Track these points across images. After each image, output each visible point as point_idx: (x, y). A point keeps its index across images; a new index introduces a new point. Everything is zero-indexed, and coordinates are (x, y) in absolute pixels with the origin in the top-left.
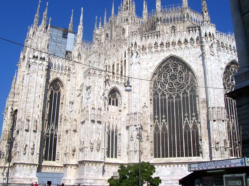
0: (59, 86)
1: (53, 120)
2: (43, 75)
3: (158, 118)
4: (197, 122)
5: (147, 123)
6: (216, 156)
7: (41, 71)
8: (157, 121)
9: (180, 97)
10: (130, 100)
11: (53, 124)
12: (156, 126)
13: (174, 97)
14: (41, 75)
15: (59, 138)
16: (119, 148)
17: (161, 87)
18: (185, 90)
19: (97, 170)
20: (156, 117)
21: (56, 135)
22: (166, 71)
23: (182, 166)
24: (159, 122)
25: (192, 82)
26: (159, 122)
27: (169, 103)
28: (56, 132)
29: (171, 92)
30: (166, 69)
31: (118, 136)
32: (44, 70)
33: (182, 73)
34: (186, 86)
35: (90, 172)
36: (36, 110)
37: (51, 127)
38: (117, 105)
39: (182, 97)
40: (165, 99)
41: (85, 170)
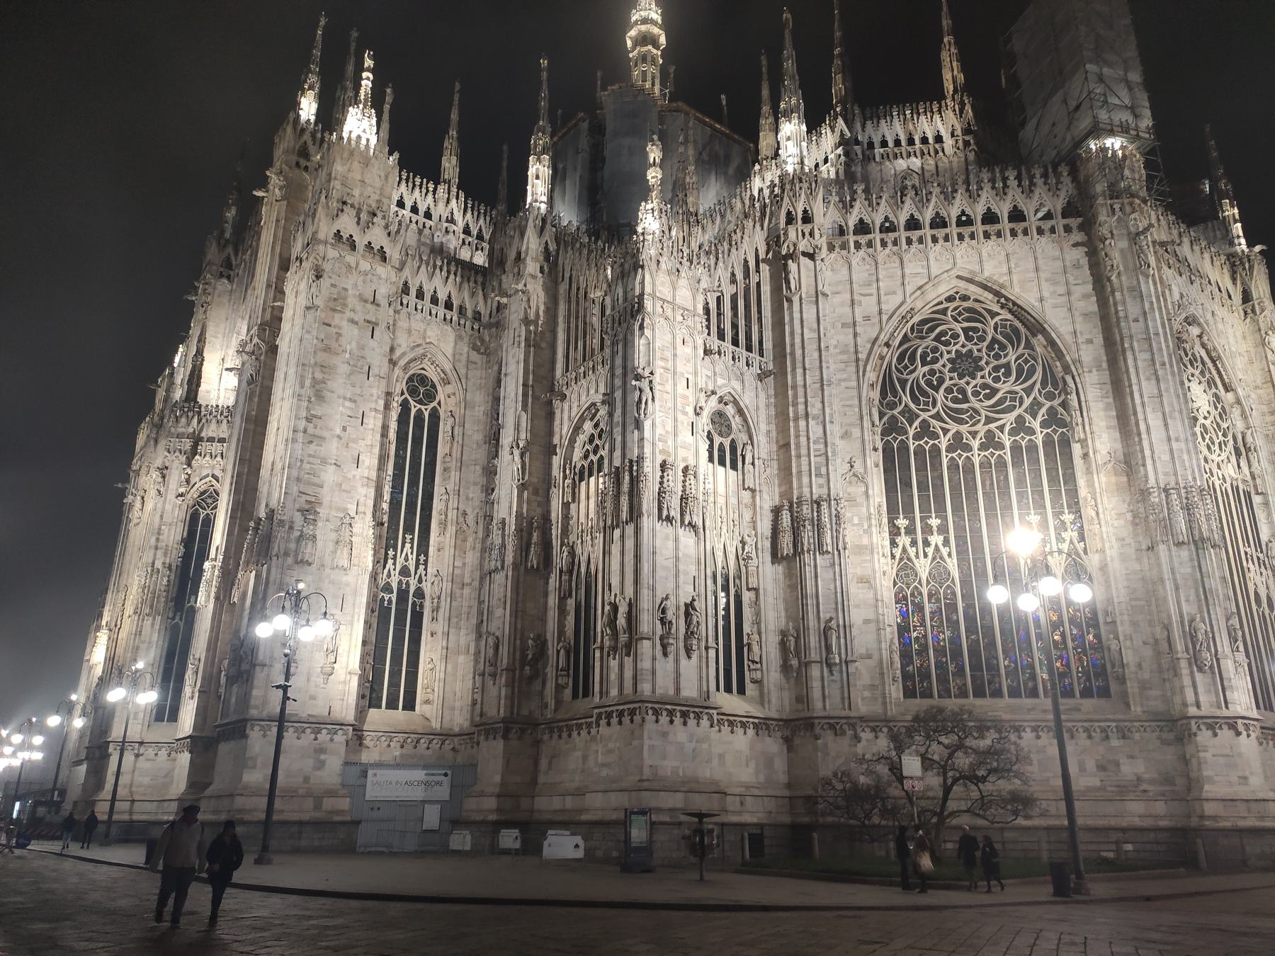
0: (434, 386)
1: (409, 529)
2: (377, 324)
3: (910, 530)
4: (1085, 551)
5: (866, 547)
6: (1202, 698)
7: (369, 306)
8: (904, 540)
9: (1000, 446)
10: (793, 446)
11: (408, 546)
12: (901, 559)
13: (976, 444)
14: (369, 322)
15: (436, 609)
16: (755, 648)
17: (915, 400)
18: (1020, 416)
19: (693, 744)
20: (902, 522)
21: (420, 594)
22: (933, 335)
23: (1038, 737)
24: (914, 543)
25: (1049, 388)
26: (914, 543)
27: (953, 466)
28: (420, 581)
29: (961, 422)
30: (931, 330)
31: (747, 597)
32: (384, 302)
33: (1003, 347)
34: (1027, 402)
35: (664, 757)
36: (350, 476)
37: (400, 561)
38: (734, 467)
39: (1008, 444)
40: (936, 451)
41: (646, 747)
